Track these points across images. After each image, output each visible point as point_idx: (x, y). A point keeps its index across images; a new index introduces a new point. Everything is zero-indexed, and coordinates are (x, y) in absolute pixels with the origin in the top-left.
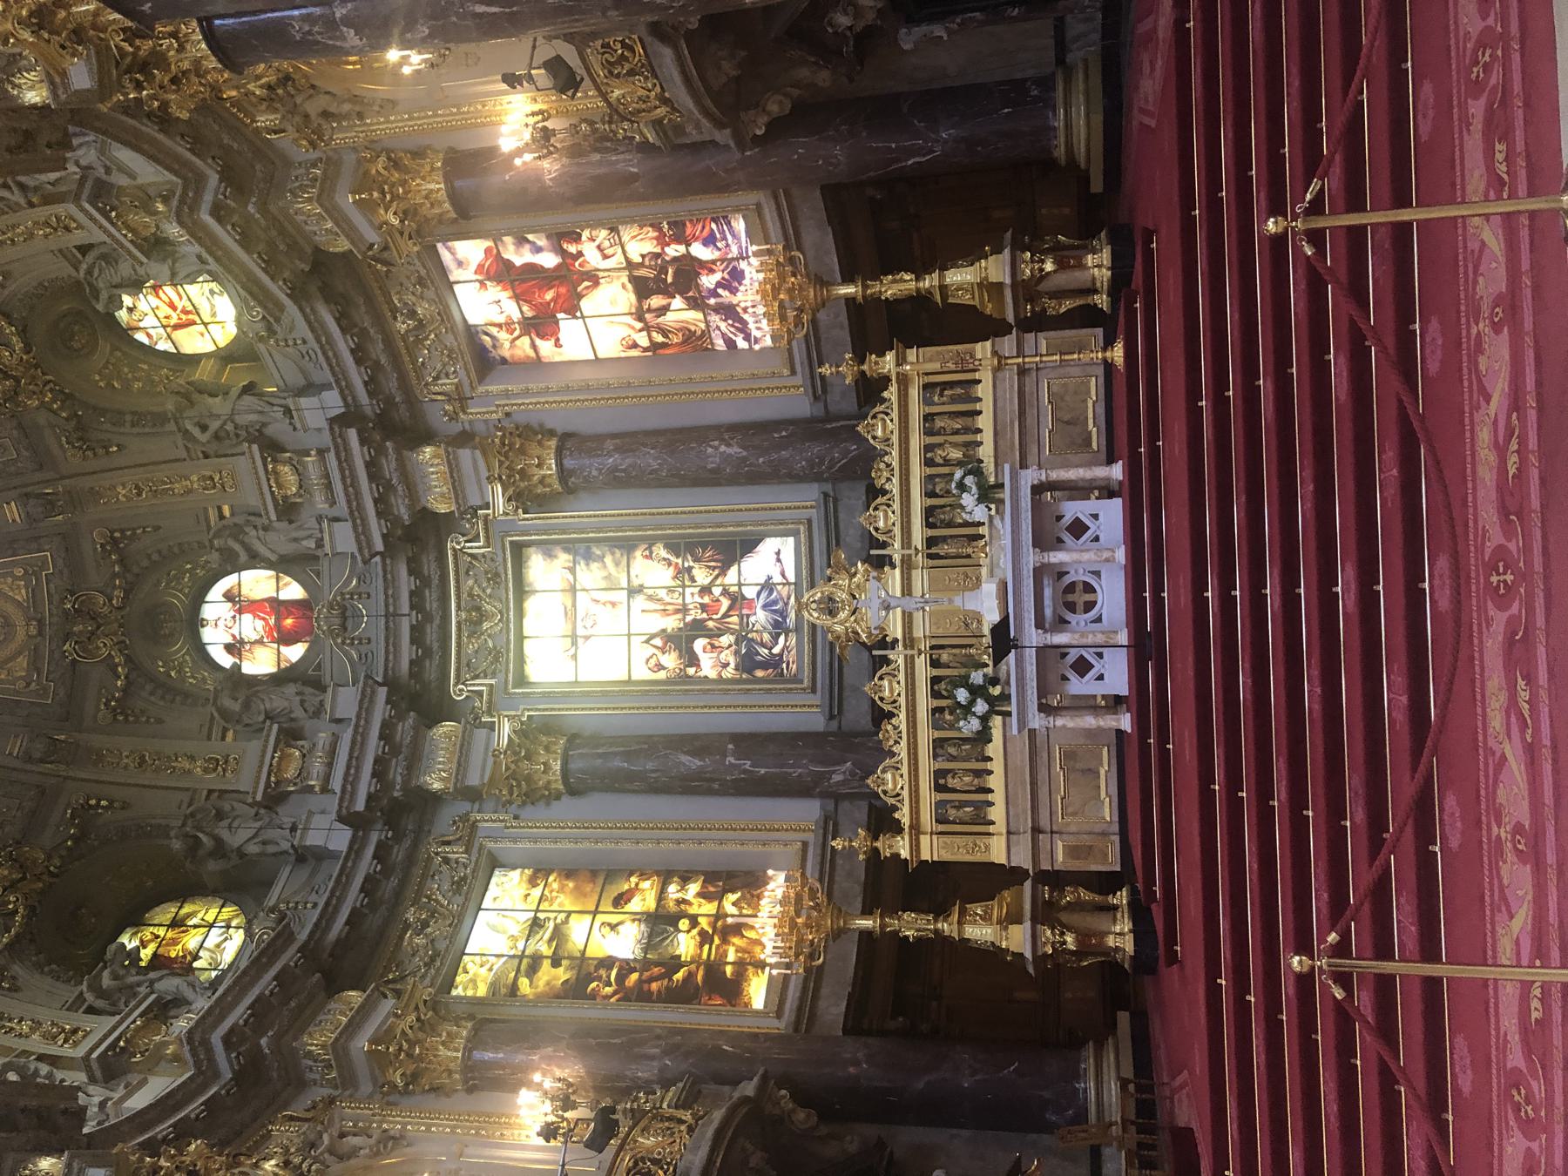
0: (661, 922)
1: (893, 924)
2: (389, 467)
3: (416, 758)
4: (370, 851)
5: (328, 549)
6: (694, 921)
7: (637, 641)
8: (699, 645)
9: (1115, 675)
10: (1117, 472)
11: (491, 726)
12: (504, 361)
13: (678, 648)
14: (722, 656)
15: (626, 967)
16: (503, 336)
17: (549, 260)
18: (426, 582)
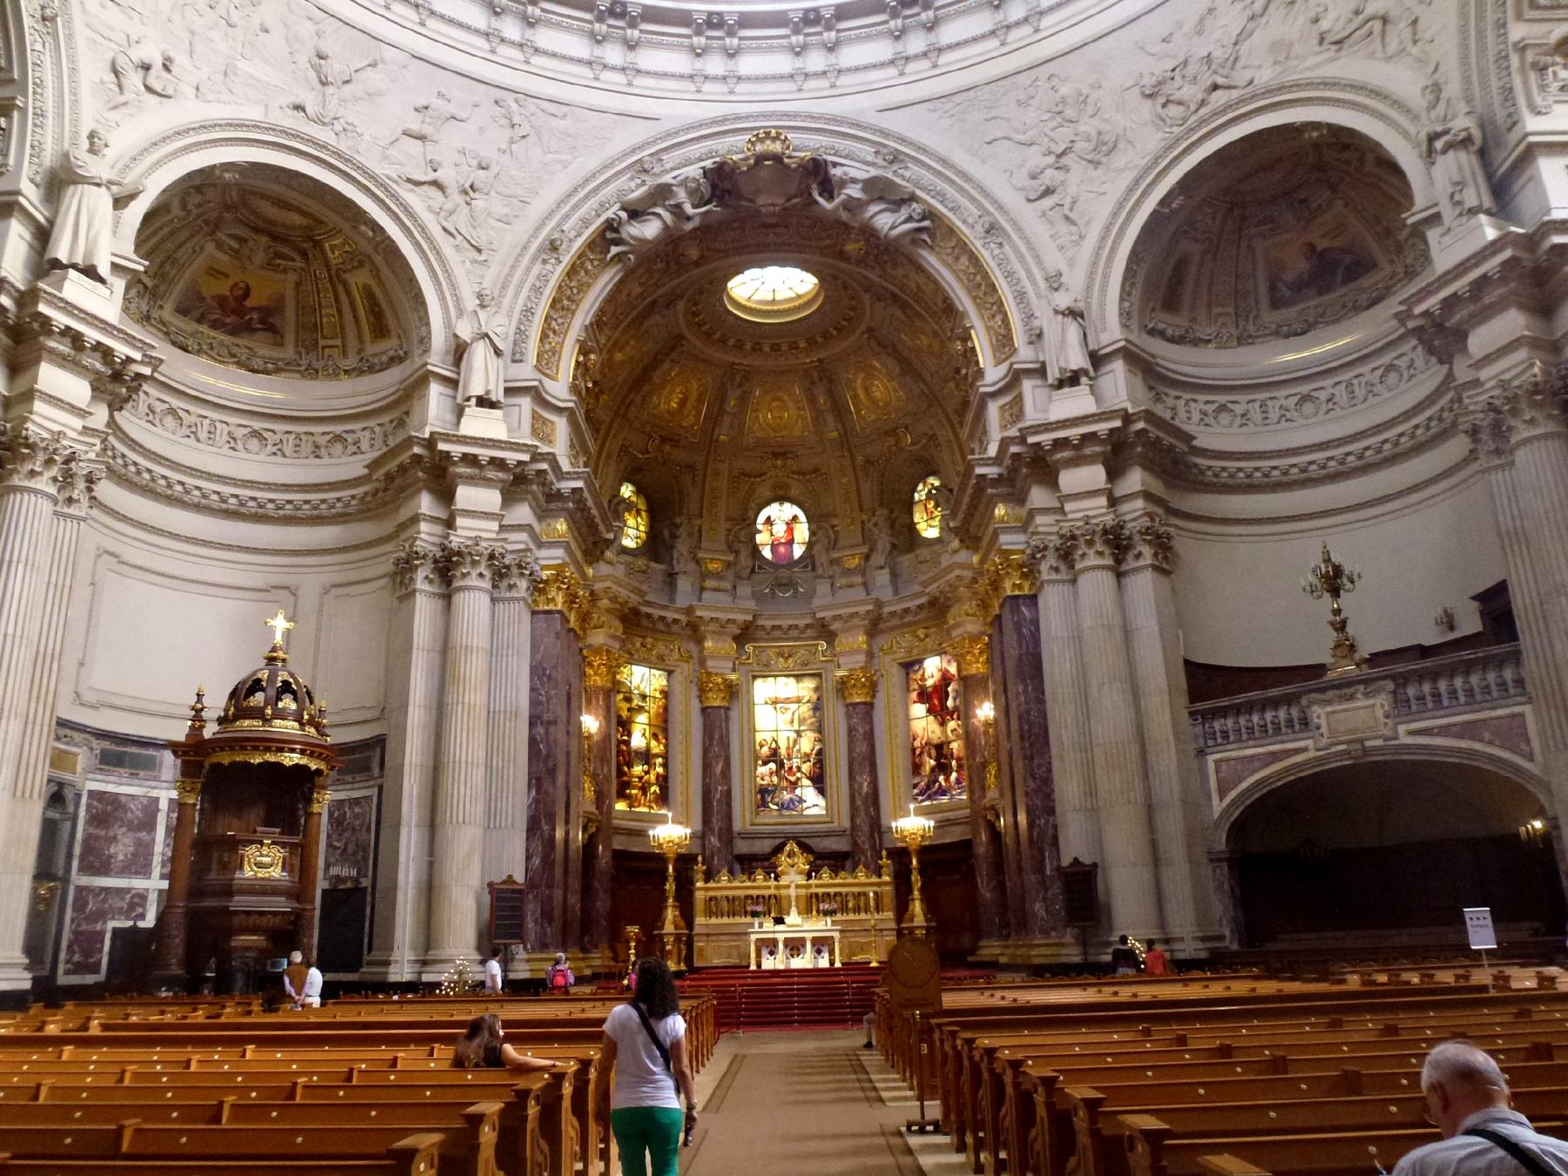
0: (646, 757)
1: (671, 879)
2: (856, 621)
3: (720, 634)
4: (677, 616)
5: (819, 581)
6: (647, 773)
7: (774, 734)
8: (772, 766)
9: (769, 963)
10: (838, 965)
11: (734, 670)
12: (908, 674)
13: (772, 755)
14: (767, 778)
15: (627, 743)
16: (918, 676)
17: (950, 703)
18: (803, 632)
